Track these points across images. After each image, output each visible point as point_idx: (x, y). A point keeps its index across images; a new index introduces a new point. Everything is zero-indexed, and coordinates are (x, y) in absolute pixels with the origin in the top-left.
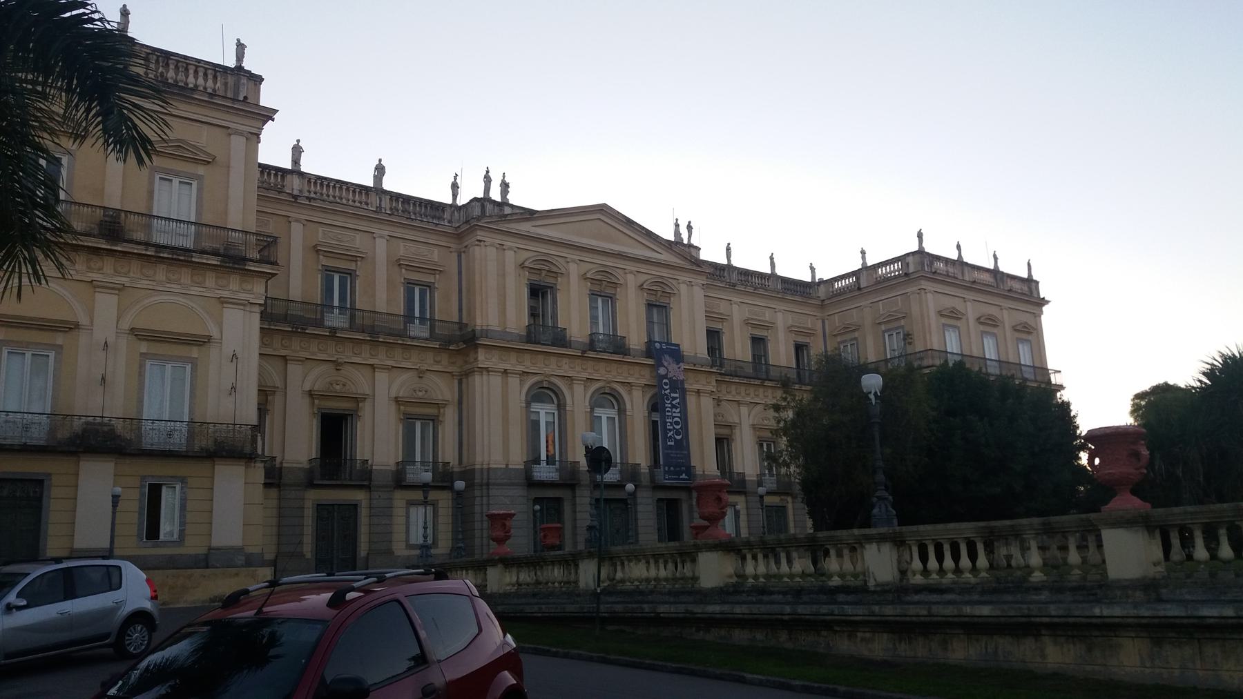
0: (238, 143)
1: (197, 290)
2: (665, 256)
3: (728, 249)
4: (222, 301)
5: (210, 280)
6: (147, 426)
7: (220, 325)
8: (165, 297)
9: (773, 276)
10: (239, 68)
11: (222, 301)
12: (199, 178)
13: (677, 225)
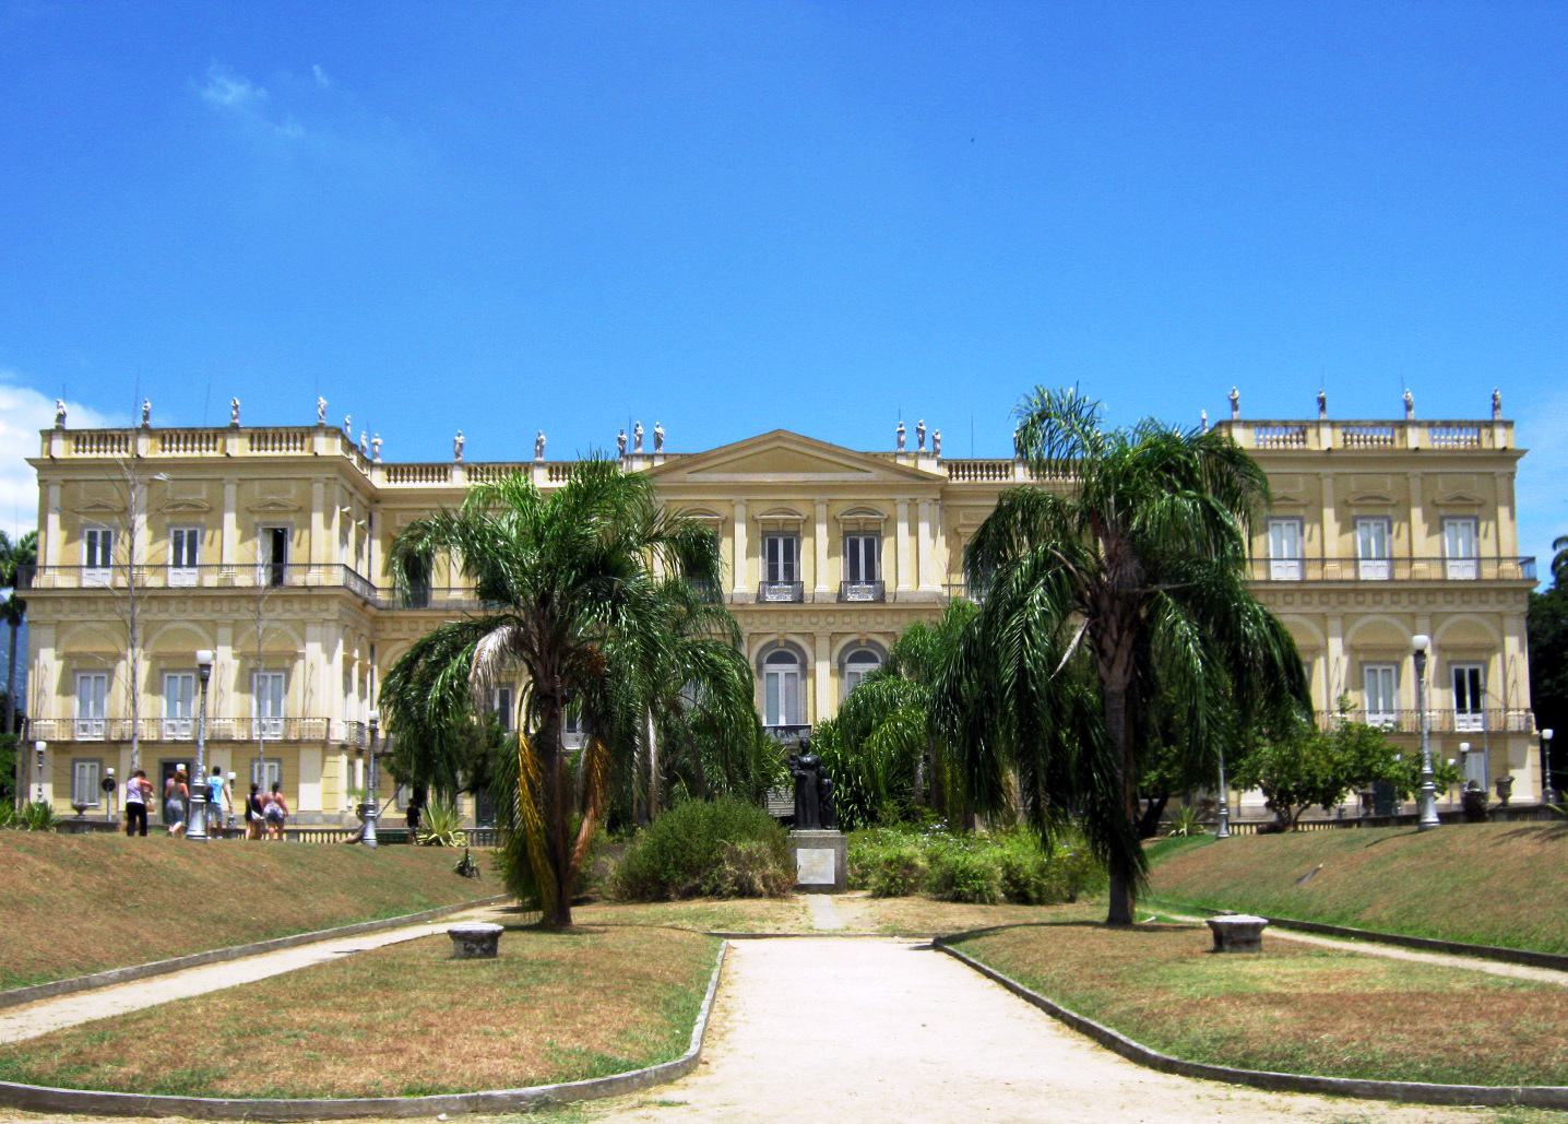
1: (288, 616)
2: (874, 475)
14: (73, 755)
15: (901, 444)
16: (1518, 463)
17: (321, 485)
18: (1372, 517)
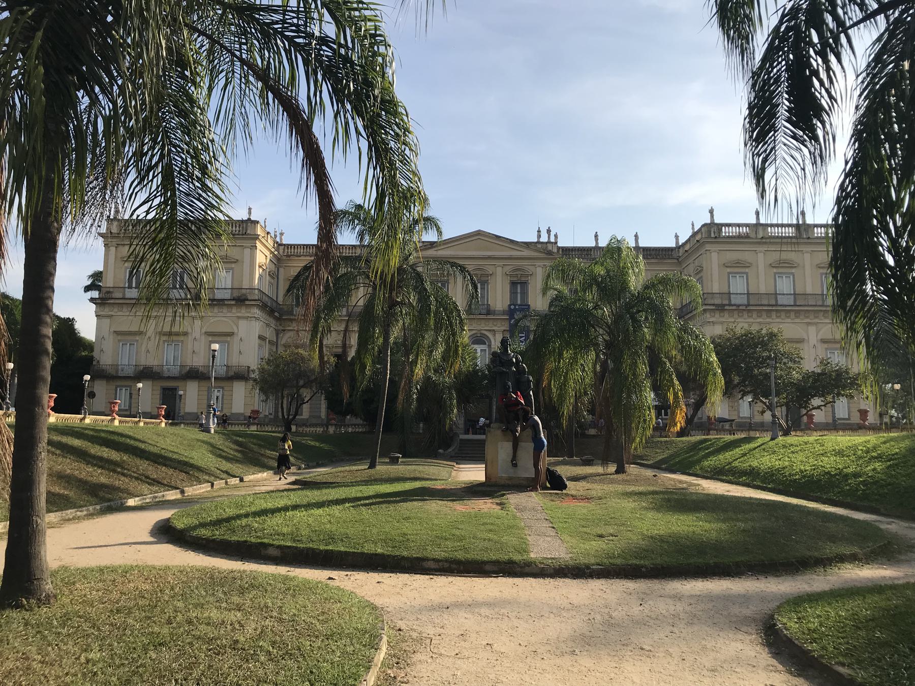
0: (247, 251)
1: (229, 315)
2: (526, 253)
3: (596, 236)
4: (239, 318)
10: (249, 219)
11: (239, 318)
12: (232, 269)
13: (539, 231)
15: (539, 236)
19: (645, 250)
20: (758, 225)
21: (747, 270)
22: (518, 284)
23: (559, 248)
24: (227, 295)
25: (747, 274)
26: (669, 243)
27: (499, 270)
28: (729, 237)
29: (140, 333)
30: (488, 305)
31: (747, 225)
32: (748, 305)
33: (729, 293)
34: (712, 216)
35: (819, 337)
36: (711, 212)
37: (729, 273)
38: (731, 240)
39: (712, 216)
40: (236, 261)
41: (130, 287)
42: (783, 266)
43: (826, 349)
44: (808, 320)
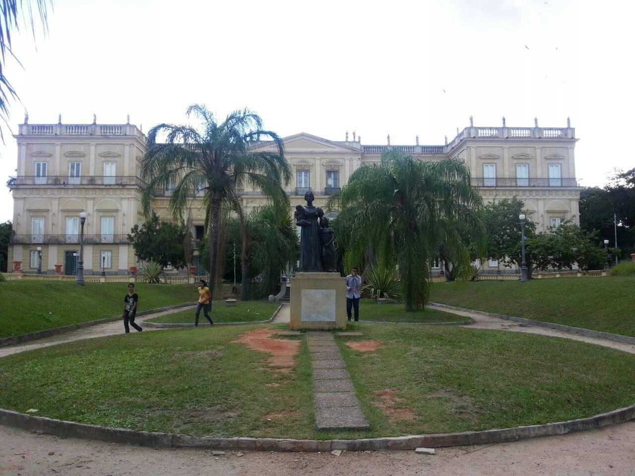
1: (114, 196)
4: (122, 198)
5: (118, 192)
6: (103, 237)
7: (121, 205)
8: (106, 199)
9: (418, 146)
11: (122, 198)
12: (116, 161)
14: (30, 249)
15: (347, 137)
16: (577, 143)
17: (128, 147)
18: (522, 163)
19: (424, 148)
20: (504, 128)
21: (496, 161)
22: (332, 172)
23: (361, 146)
24: (113, 182)
25: (496, 164)
26: (442, 143)
27: (318, 162)
28: (483, 137)
29: (48, 211)
30: (310, 188)
31: (497, 129)
32: (496, 186)
33: (483, 178)
34: (472, 122)
35: (546, 209)
36: (471, 119)
37: (483, 164)
38: (485, 139)
39: (472, 122)
40: (119, 156)
41: (38, 176)
42: (522, 159)
43: (551, 217)
44: (538, 197)
